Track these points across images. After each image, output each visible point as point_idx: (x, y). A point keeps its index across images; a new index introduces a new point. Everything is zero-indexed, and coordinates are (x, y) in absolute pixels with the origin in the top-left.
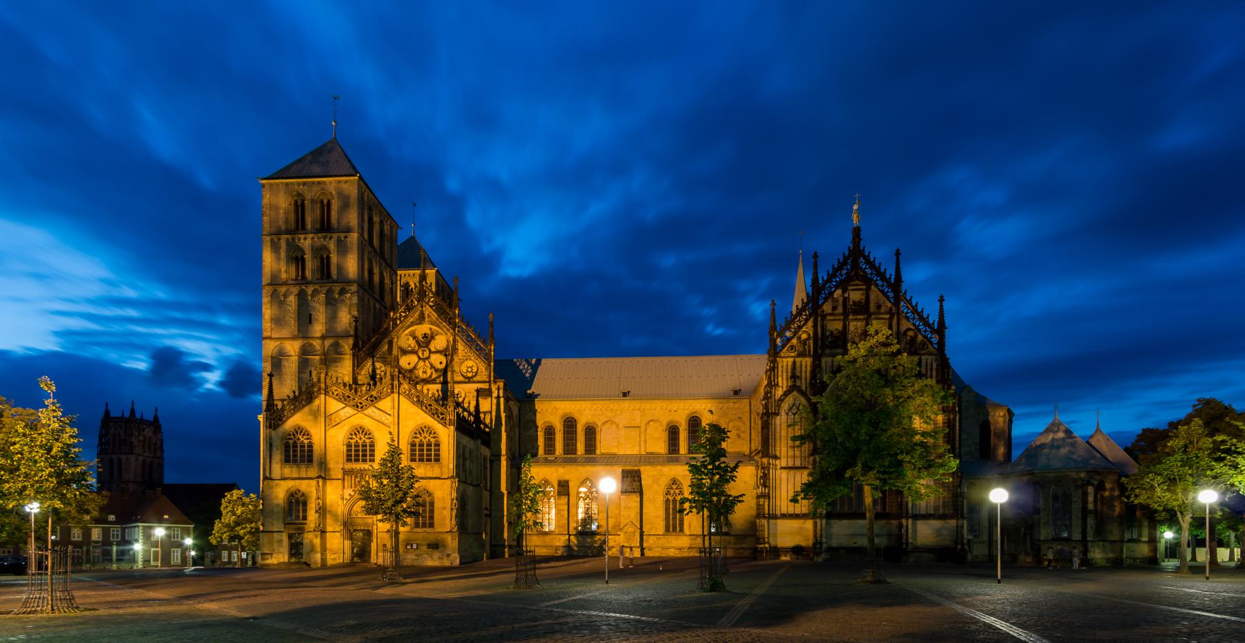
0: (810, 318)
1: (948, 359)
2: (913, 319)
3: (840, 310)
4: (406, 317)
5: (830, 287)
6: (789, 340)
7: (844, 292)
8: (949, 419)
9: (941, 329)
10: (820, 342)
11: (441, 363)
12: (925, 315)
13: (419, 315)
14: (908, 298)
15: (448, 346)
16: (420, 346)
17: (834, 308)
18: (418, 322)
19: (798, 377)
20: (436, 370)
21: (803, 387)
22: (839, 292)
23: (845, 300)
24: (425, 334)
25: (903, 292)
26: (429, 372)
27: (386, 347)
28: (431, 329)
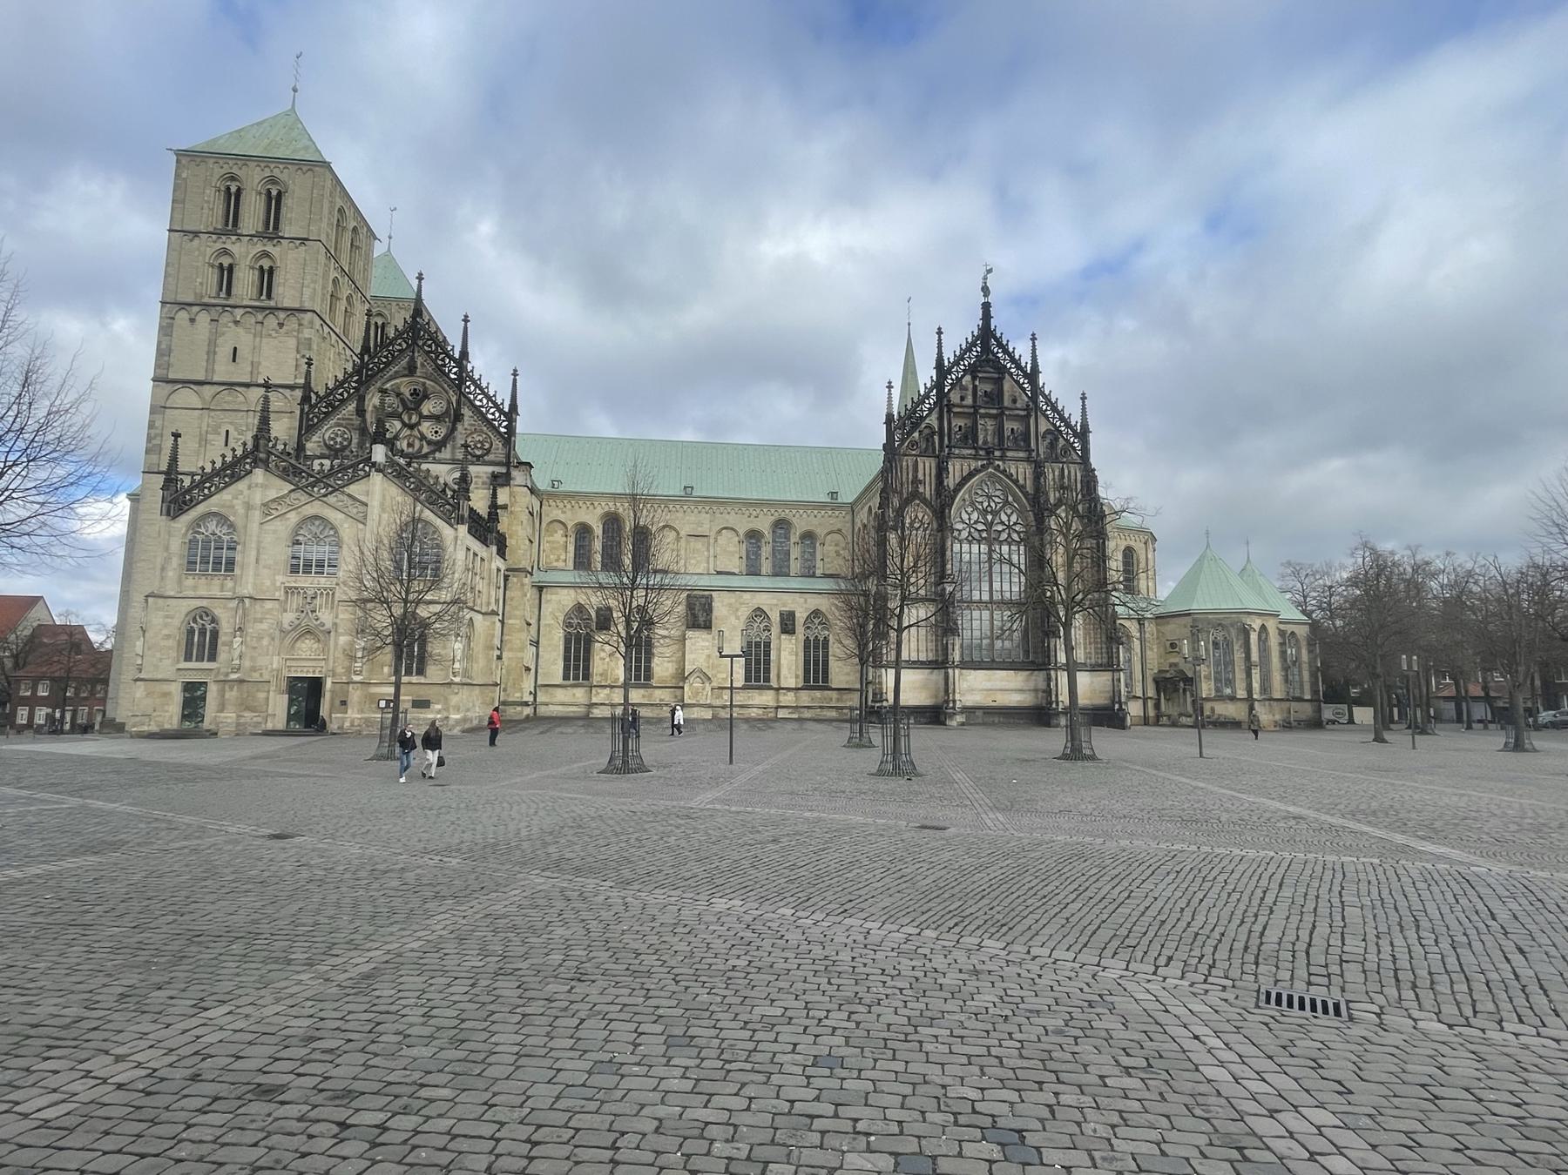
0: (934, 409)
1: (1094, 470)
2: (1054, 418)
3: (969, 401)
4: (388, 364)
5: (957, 371)
6: (910, 433)
7: (974, 378)
8: (1098, 543)
9: (1083, 435)
10: (946, 438)
11: (436, 432)
12: (1066, 416)
13: (408, 362)
14: (1047, 392)
15: (448, 409)
16: (406, 408)
17: (962, 399)
18: (406, 372)
19: (920, 482)
20: (429, 443)
21: (928, 496)
22: (968, 378)
23: (975, 387)
24: (415, 390)
25: (1041, 385)
26: (417, 444)
27: (354, 405)
28: (424, 384)
